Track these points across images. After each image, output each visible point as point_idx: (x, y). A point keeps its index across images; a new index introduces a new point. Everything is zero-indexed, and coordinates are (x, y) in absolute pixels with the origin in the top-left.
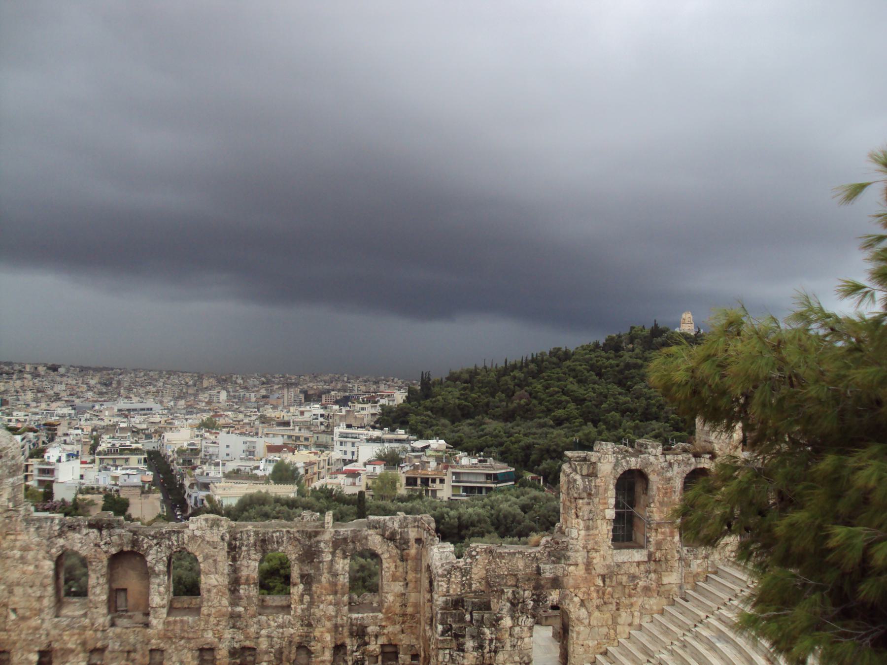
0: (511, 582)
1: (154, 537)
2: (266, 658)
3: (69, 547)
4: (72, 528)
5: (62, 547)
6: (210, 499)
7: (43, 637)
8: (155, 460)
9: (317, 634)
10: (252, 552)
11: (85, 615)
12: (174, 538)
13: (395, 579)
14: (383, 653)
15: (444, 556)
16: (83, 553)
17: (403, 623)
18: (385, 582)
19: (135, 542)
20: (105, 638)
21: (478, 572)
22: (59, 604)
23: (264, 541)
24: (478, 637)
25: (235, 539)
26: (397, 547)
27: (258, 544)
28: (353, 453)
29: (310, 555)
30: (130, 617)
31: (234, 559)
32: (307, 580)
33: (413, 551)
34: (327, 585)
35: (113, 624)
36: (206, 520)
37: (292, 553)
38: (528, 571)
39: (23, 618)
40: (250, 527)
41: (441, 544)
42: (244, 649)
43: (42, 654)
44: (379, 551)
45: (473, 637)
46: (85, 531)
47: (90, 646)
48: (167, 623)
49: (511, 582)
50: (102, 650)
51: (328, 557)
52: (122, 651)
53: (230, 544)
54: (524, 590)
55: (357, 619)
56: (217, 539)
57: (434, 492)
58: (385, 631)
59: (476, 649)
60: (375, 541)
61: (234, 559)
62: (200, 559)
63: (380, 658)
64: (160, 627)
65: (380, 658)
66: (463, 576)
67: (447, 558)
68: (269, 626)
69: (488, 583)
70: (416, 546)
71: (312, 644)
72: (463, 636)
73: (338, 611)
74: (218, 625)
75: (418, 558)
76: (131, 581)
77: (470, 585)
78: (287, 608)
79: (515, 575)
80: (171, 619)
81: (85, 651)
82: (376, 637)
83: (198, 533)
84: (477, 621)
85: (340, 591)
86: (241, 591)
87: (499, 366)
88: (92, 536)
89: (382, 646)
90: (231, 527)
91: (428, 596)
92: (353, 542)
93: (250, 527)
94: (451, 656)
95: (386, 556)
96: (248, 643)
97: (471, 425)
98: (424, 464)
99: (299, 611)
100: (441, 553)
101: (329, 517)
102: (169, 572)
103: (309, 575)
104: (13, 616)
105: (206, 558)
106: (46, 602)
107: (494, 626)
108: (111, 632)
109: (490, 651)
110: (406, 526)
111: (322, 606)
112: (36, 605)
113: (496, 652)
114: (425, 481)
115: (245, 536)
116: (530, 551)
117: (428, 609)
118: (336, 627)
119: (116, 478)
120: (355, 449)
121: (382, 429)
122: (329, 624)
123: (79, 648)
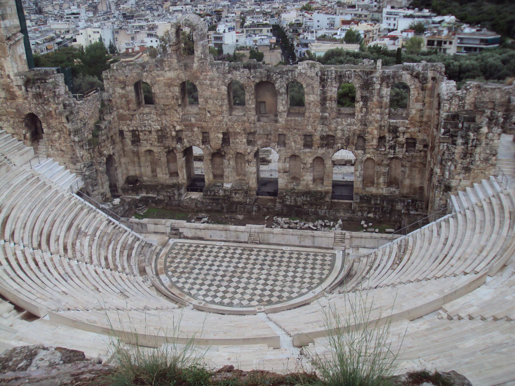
0: (490, 106)
1: (279, 73)
2: (340, 141)
3: (234, 79)
4: (235, 68)
5: (231, 79)
6: (308, 52)
8: (277, 30)
9: (369, 130)
10: (334, 82)
11: (244, 115)
12: (290, 74)
13: (417, 101)
14: (407, 143)
15: (449, 88)
16: (242, 82)
17: (420, 126)
18: (411, 102)
19: (268, 76)
20: (255, 127)
21: (469, 99)
22: (231, 109)
23: (340, 76)
24: (466, 137)
25: (324, 75)
26: (420, 82)
27: (337, 78)
28: (394, 25)
29: (367, 85)
30: (267, 117)
31: (323, 87)
32: (365, 99)
33: (429, 85)
34: (376, 103)
35: (259, 120)
36: (308, 64)
37: (356, 83)
38: (503, 100)
39: (214, 116)
40: (333, 68)
41: (448, 81)
42: (328, 136)
43: (224, 134)
44: (409, 84)
45: (462, 137)
46: (242, 70)
47: (248, 131)
48: (287, 121)
49: (490, 106)
50: (254, 133)
51: (377, 87)
52: (264, 134)
53: (321, 78)
54: (499, 112)
55: (393, 123)
56: (314, 75)
57: (445, 50)
58: (409, 131)
59: (463, 144)
60: (406, 78)
61: (323, 87)
62: (304, 86)
63: (405, 145)
64: (284, 122)
65: (405, 145)
66: (460, 101)
67: (451, 90)
68: (342, 124)
69: (476, 107)
70: (432, 81)
72: (456, 136)
73: (382, 118)
74: (314, 122)
75: (433, 89)
76: (268, 98)
77: (464, 107)
78: (353, 115)
79: (494, 102)
80: (289, 118)
81: (245, 134)
82: (404, 133)
83: (303, 71)
84: (466, 128)
85: (384, 106)
86: (327, 105)
88: (246, 73)
89: (407, 139)
90: (321, 68)
91: (437, 112)
92: (393, 78)
93: (333, 68)
94: (448, 147)
95: (413, 87)
96: (330, 133)
97: (473, 6)
98: (440, 32)
99: (360, 117)
100: (447, 87)
101: (379, 63)
102: (287, 93)
103: (366, 96)
104: (209, 115)
105: (308, 85)
106: (224, 108)
107: (476, 131)
108: (258, 124)
109: (472, 146)
111: (373, 115)
112: (219, 109)
113: (475, 146)
114: (440, 43)
115: (329, 74)
116: (506, 88)
117: (436, 119)
118: (381, 126)
119: (255, 41)
120: (395, 22)
121: (413, 9)
122: (376, 125)
123: (242, 132)
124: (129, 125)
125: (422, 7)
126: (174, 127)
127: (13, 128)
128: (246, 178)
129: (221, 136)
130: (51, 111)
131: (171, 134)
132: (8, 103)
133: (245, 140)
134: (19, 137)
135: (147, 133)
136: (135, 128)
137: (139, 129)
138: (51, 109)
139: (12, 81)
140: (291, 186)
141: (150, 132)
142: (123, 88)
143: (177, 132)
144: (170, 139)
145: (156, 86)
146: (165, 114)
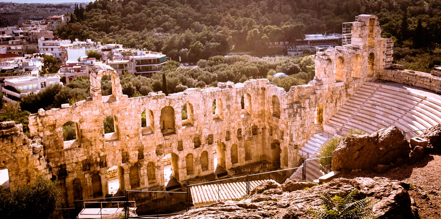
7: (140, 144)
9: (233, 126)
12: (183, 99)
19: (170, 103)
31: (205, 104)
39: (132, 138)
42: (209, 135)
43: (139, 150)
61: (205, 104)
62: (193, 105)
70: (261, 90)
71: (231, 129)
75: (263, 94)
86: (208, 115)
93: (208, 91)
95: (253, 94)
96: (210, 133)
104: (128, 138)
110: (258, 84)
124: (58, 162)
126: (99, 154)
128: (155, 181)
129: (137, 152)
131: (96, 161)
133: (155, 151)
135: (74, 165)
136: (63, 163)
137: (67, 162)
138: (22, 156)
140: (189, 177)
141: (76, 163)
142: (51, 131)
144: (95, 165)
145: (84, 124)
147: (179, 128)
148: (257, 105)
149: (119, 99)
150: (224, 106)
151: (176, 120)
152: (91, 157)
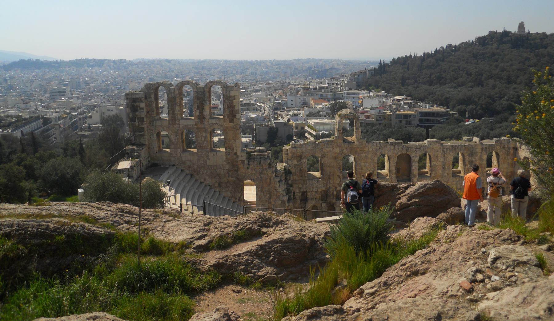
10: (451, 153)
12: (422, 148)
19: (407, 151)
31: (444, 156)
61: (444, 156)
87: (418, 55)
93: (449, 144)
114: (406, 116)
120: (353, 100)
124: (300, 188)
125: (370, 88)
126: (336, 188)
127: (231, 193)
130: (267, 179)
131: (333, 193)
132: (230, 173)
134: (233, 200)
135: (314, 193)
136: (305, 190)
139: (238, 157)
141: (316, 192)
143: (337, 191)
144: (332, 197)
146: (330, 179)
147: (415, 176)
148: (506, 165)
149: (358, 141)
150: (467, 162)
151: (413, 168)
152: (328, 189)
